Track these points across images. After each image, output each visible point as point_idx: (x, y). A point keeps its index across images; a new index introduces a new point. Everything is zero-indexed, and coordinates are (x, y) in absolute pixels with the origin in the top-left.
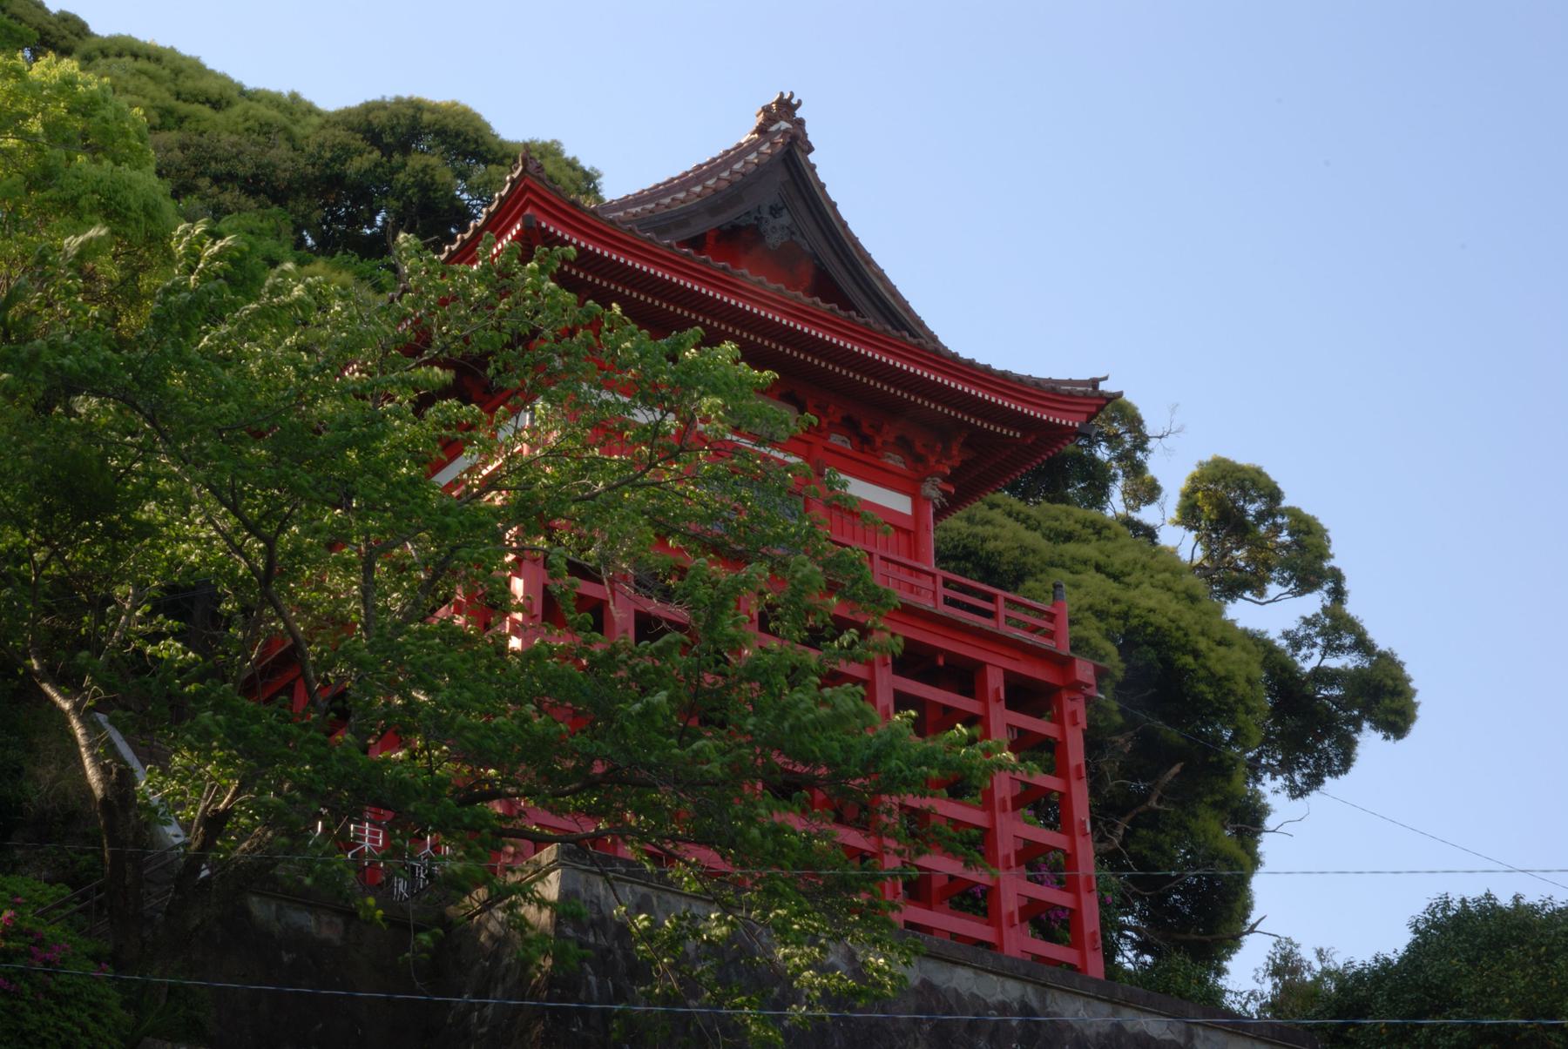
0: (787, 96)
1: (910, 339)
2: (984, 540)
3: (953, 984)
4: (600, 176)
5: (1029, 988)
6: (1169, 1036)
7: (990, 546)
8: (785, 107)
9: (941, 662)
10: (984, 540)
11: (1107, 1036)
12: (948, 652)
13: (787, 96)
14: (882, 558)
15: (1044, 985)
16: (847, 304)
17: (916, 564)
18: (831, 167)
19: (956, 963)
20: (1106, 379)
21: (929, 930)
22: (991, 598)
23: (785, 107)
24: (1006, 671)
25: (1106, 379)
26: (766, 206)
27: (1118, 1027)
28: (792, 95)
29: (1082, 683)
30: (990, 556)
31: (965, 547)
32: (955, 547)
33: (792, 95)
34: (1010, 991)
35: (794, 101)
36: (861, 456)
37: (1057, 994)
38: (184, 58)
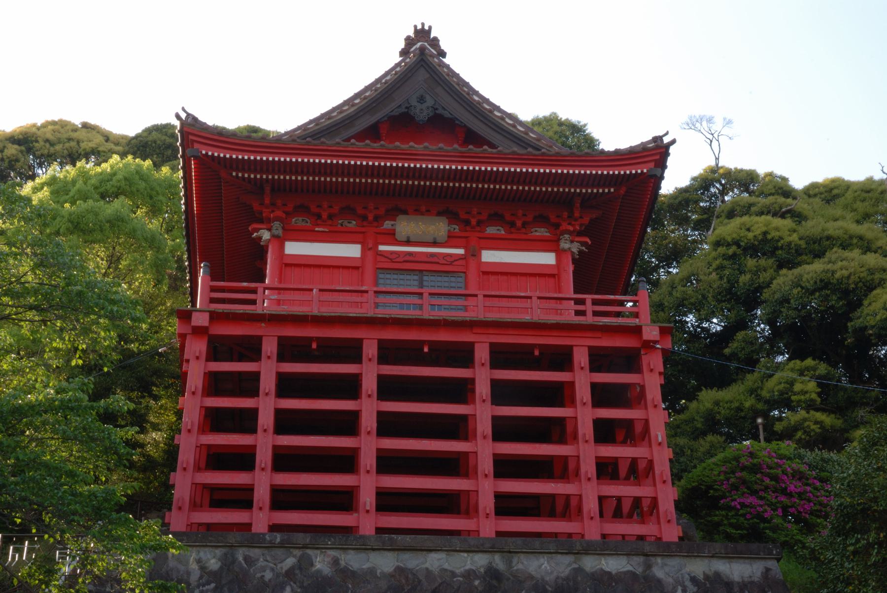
0: (419, 27)
1: (490, 150)
2: (833, 272)
3: (427, 565)
4: (585, 125)
5: (497, 558)
6: (630, 568)
7: (838, 275)
8: (423, 34)
9: (426, 350)
10: (833, 272)
11: (567, 579)
12: (539, 345)
13: (419, 27)
14: (539, 298)
15: (510, 552)
16: (360, 137)
17: (560, 295)
18: (463, 60)
19: (430, 551)
20: (667, 133)
21: (556, 535)
22: (254, 291)
23: (423, 34)
24: (590, 348)
25: (667, 133)
26: (421, 99)
27: (579, 570)
28: (423, 24)
29: (649, 341)
30: (840, 281)
31: (821, 281)
32: (816, 283)
33: (423, 24)
34: (479, 561)
35: (426, 28)
36: (513, 236)
37: (522, 556)
38: (137, 137)
